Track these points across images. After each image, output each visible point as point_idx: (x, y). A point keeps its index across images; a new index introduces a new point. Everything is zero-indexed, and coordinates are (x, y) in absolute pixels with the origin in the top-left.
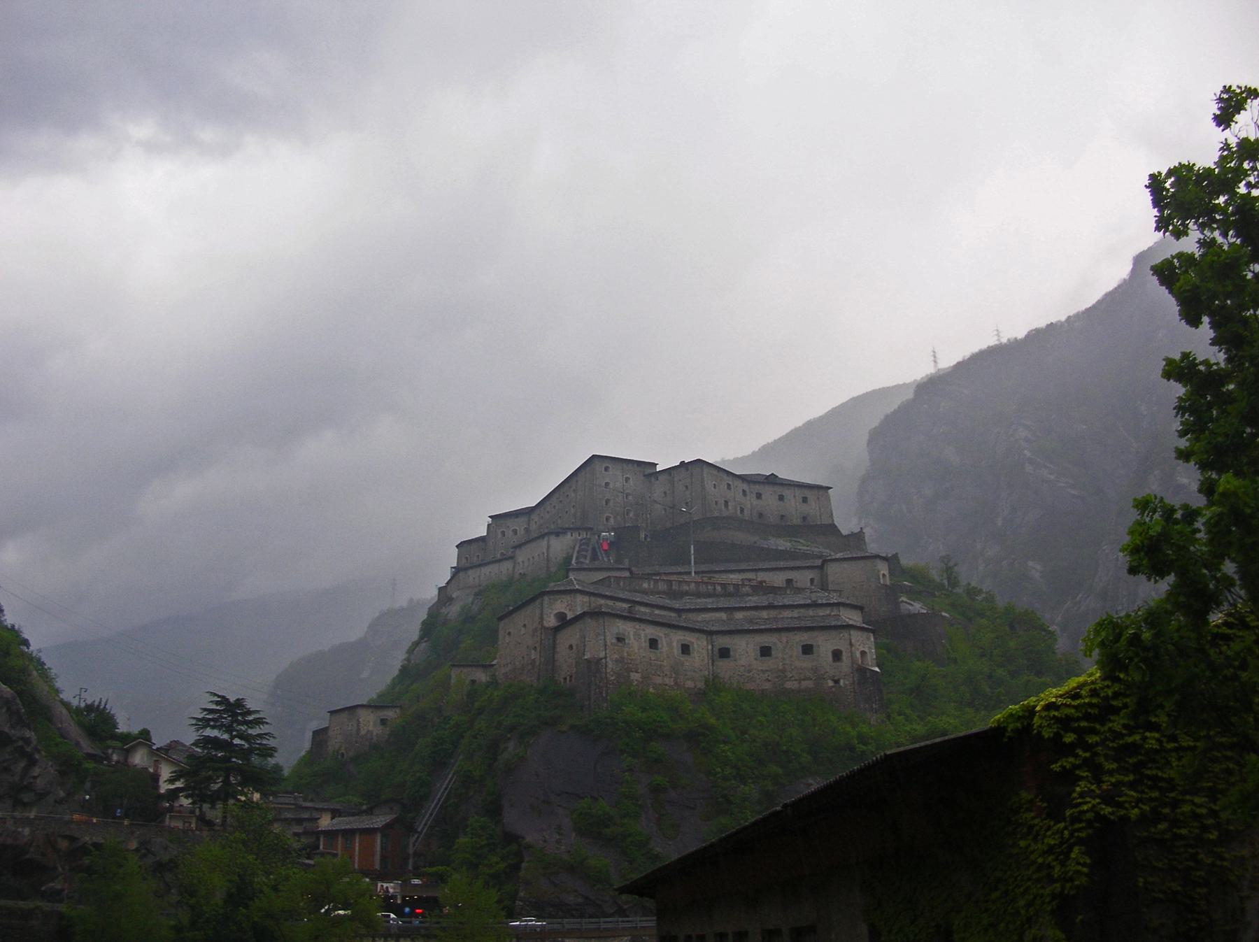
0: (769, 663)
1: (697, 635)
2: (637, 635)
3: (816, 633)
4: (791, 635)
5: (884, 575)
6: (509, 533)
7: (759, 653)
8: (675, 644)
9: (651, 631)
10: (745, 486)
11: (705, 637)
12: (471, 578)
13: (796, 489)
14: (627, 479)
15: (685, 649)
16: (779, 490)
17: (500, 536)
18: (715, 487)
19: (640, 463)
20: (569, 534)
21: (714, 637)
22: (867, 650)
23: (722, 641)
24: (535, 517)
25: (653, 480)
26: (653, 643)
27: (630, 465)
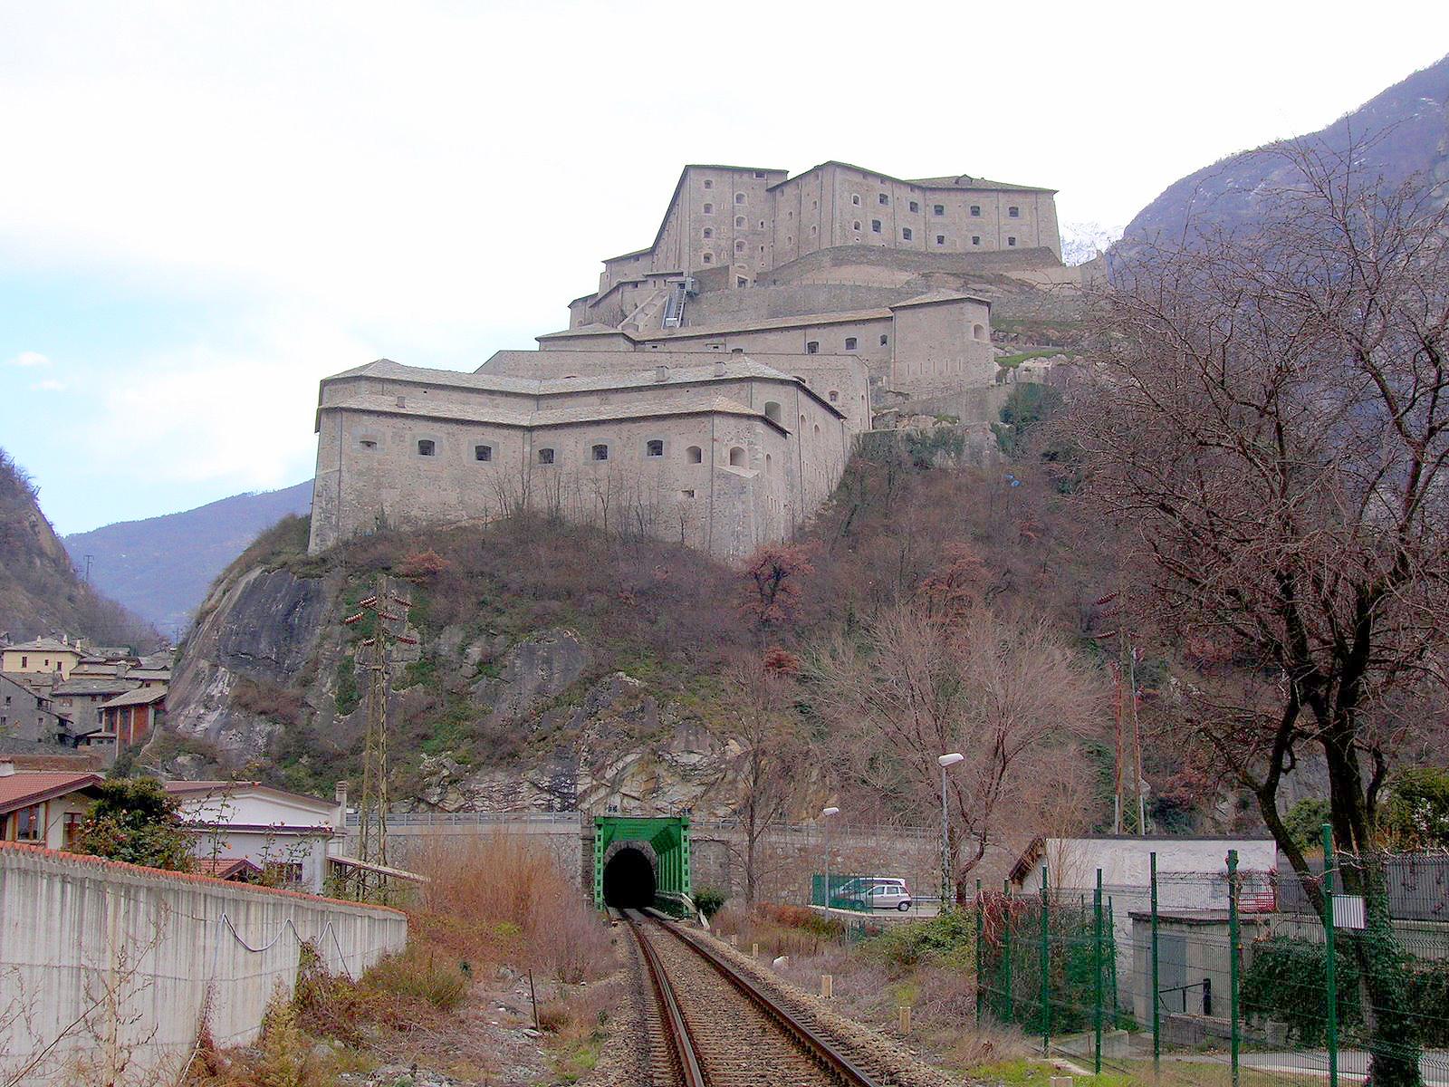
1: (506, 432)
3: (667, 424)
5: (977, 329)
10: (916, 196)
11: (519, 433)
13: (1001, 195)
14: (739, 198)
16: (973, 199)
19: (760, 173)
21: (535, 434)
22: (745, 447)
23: (545, 440)
25: (778, 192)
27: (746, 177)
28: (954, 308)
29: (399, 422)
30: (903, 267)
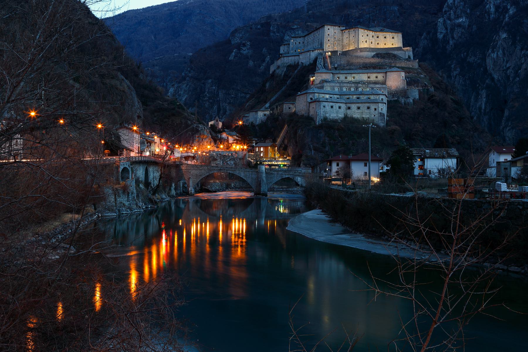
0: (359, 111)
1: (342, 104)
2: (328, 106)
3: (370, 104)
4: (365, 104)
5: (403, 76)
6: (298, 43)
7: (357, 108)
8: (337, 107)
9: (331, 104)
12: (285, 60)
15: (340, 107)
17: (294, 44)
18: (362, 36)
20: (316, 51)
23: (349, 105)
24: (306, 38)
26: (332, 107)
27: (336, 27)
28: (399, 73)
29: (328, 103)
30: (373, 52)
